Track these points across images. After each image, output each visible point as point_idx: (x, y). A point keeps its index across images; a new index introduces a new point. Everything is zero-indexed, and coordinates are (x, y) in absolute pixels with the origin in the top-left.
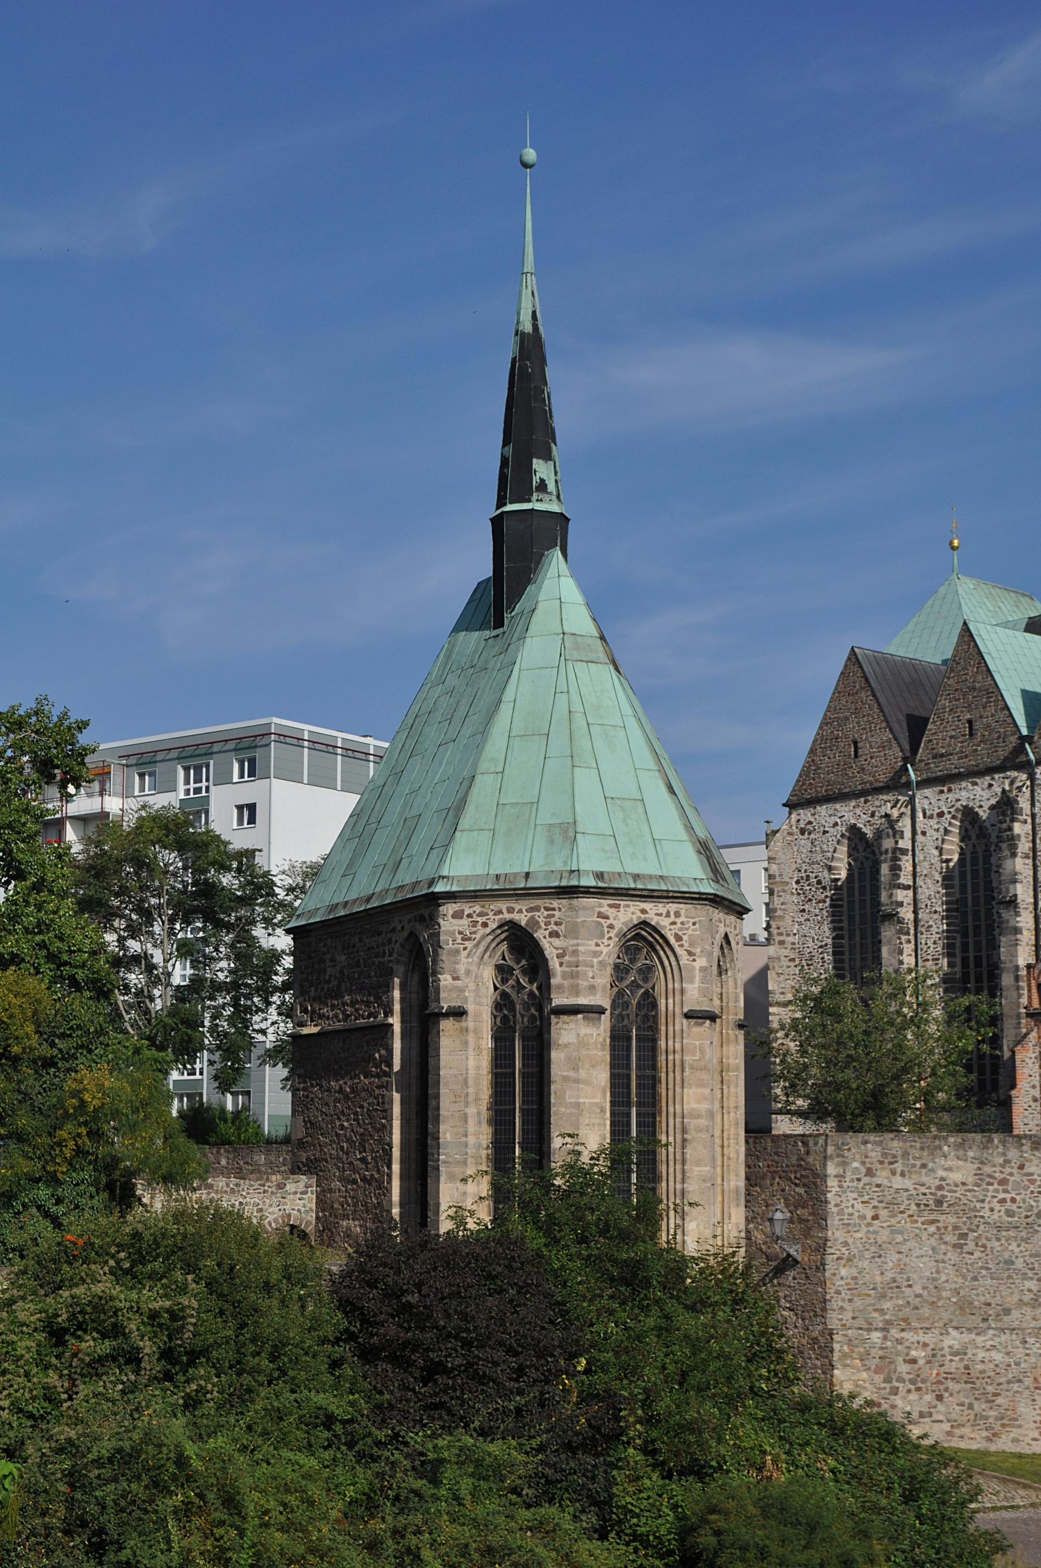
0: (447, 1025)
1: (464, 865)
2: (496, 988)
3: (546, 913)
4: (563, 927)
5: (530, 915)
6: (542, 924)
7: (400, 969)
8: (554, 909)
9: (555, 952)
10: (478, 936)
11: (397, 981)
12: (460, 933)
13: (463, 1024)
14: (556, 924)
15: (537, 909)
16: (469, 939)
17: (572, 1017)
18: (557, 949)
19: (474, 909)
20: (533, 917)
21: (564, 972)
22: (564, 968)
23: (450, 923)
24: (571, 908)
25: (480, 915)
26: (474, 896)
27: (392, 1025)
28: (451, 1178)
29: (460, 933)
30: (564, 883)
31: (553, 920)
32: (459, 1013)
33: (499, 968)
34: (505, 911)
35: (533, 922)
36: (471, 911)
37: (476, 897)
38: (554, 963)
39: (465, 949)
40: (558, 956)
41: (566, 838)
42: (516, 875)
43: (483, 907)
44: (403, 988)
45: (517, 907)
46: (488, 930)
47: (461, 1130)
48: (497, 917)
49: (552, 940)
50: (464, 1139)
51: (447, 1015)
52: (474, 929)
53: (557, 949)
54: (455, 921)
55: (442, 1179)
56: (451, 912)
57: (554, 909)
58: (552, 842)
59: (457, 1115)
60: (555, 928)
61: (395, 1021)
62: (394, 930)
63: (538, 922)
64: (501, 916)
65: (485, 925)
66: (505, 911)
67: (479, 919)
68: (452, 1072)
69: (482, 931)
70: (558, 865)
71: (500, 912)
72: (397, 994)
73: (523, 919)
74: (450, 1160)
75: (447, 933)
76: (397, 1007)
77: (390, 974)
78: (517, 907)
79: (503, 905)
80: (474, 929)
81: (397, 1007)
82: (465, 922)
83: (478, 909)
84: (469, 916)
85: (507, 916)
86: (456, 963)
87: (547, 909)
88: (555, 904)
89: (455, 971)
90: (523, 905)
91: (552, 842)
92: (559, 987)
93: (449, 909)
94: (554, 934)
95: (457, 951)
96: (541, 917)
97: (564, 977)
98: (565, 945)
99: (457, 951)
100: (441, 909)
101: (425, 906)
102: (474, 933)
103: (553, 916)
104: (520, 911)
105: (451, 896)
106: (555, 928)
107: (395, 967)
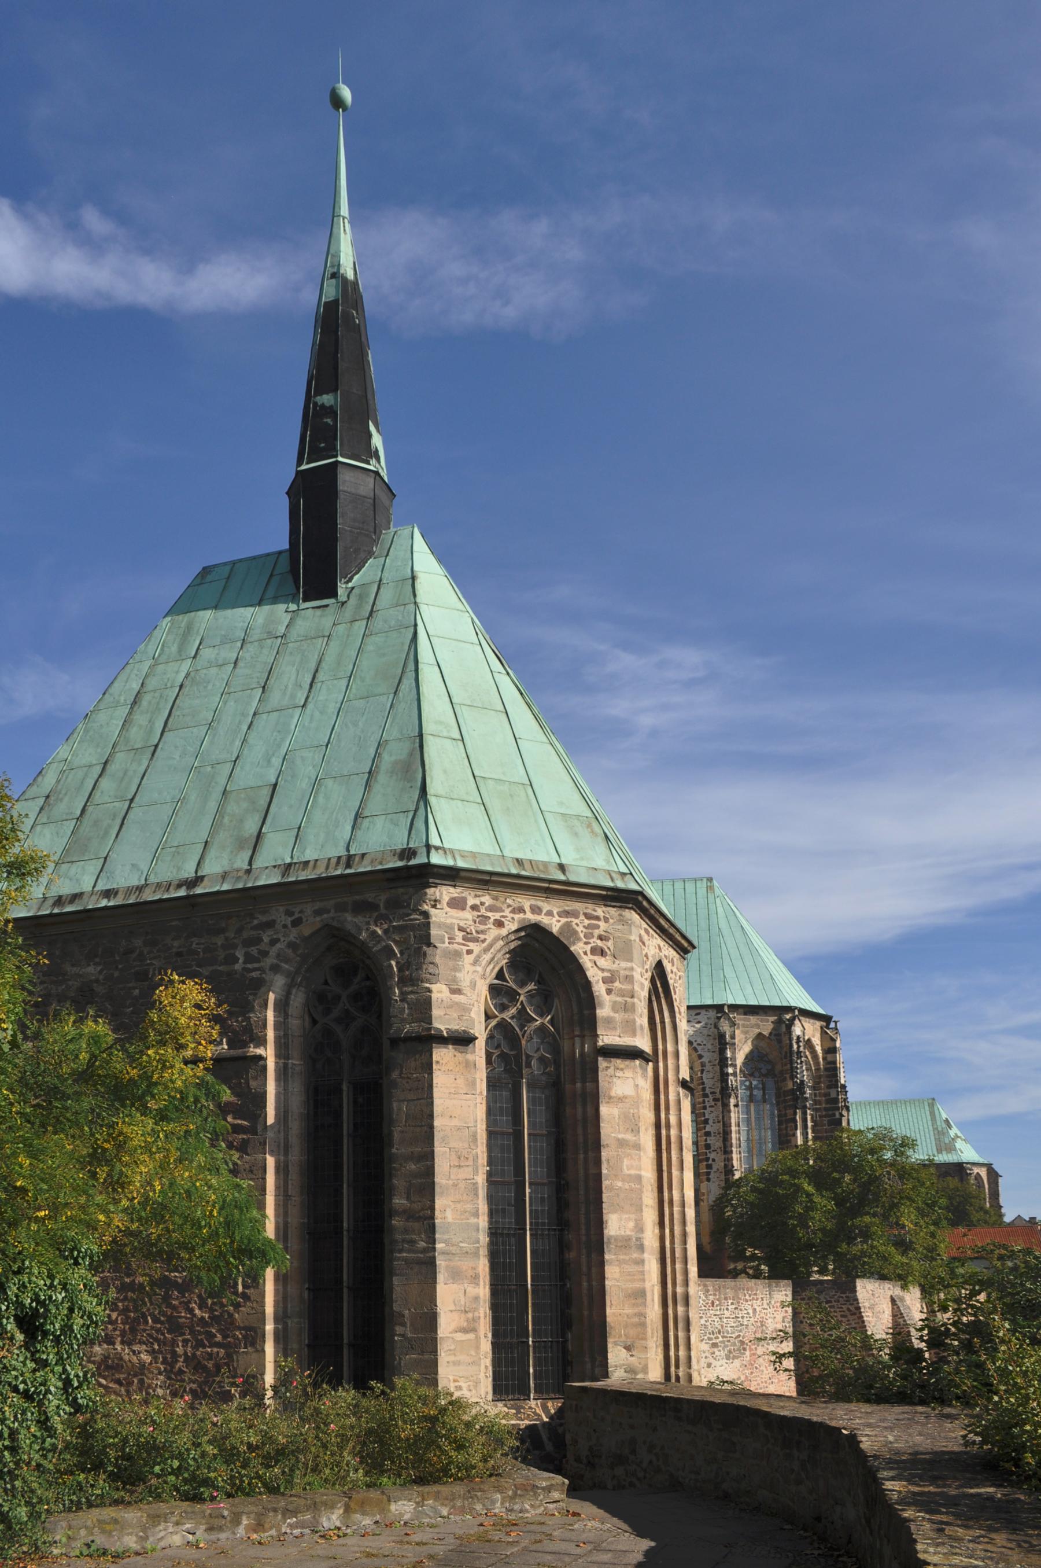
0: (443, 1056)
1: (458, 835)
2: (488, 1017)
3: (587, 922)
4: (610, 944)
5: (564, 920)
6: (582, 935)
7: (280, 981)
8: (598, 918)
9: (601, 974)
10: (490, 937)
11: (272, 997)
12: (461, 929)
13: (470, 1057)
14: (600, 938)
15: (575, 914)
16: (476, 940)
17: (628, 1062)
18: (603, 970)
19: (483, 899)
20: (568, 925)
21: (615, 1002)
22: (614, 997)
23: (446, 912)
24: (622, 920)
25: (491, 909)
27: (260, 1058)
28: (456, 1275)
30: (620, 884)
31: (596, 932)
32: (463, 1040)
33: (493, 990)
35: (567, 928)
36: (477, 901)
37: (486, 882)
38: (599, 989)
40: (605, 981)
42: (545, 864)
43: (496, 899)
44: (281, 1007)
45: (546, 907)
46: (504, 932)
47: (469, 1207)
48: (516, 916)
49: (596, 958)
50: (473, 1220)
51: (443, 1040)
52: (482, 927)
53: (603, 970)
54: (453, 912)
55: (441, 1278)
56: (446, 898)
57: (598, 918)
59: (462, 1185)
61: (269, 1053)
62: (270, 925)
63: (575, 932)
64: (522, 915)
65: (499, 924)
66: (527, 909)
67: (489, 914)
68: (455, 1122)
69: (494, 932)
71: (521, 910)
72: (270, 1015)
73: (555, 924)
74: (453, 1249)
75: (440, 926)
76: (271, 1034)
77: (259, 986)
79: (526, 902)
80: (482, 927)
81: (271, 1034)
82: (468, 915)
83: (487, 900)
85: (533, 918)
86: (457, 969)
87: (588, 916)
88: (600, 911)
89: (455, 980)
90: (555, 906)
92: (609, 1021)
93: (445, 893)
95: (457, 954)
96: (580, 925)
97: (615, 1007)
98: (615, 967)
99: (457, 954)
100: (430, 891)
101: (412, 878)
102: (483, 932)
103: (598, 927)
104: (550, 913)
105: (452, 875)
106: (599, 943)
107: (268, 977)
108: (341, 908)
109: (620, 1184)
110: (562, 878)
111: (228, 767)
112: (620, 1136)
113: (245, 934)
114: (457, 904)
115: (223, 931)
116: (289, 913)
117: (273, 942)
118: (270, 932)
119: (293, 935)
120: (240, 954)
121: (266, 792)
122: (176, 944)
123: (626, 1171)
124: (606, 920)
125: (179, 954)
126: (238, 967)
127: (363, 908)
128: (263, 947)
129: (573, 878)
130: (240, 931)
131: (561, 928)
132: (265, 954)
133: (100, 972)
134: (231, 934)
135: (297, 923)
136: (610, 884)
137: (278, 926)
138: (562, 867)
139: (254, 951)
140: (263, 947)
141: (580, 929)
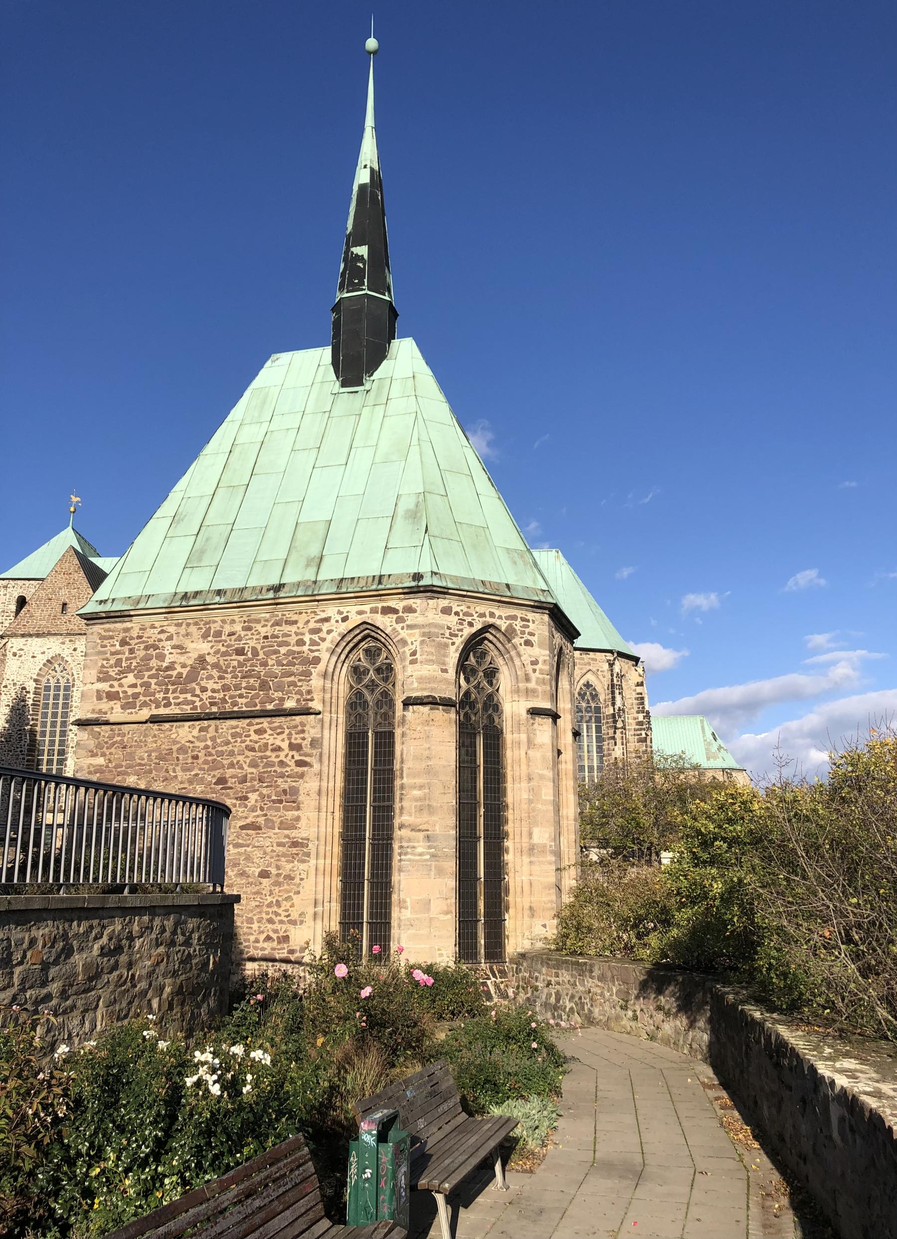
5: (508, 622)
6: (519, 632)
15: (514, 618)
16: (456, 636)
20: (511, 625)
26: (463, 595)
29: (449, 628)
31: (527, 630)
34: (487, 614)
39: (453, 644)
41: (525, 563)
48: (481, 619)
52: (461, 627)
57: (528, 621)
58: (515, 563)
60: (530, 638)
62: (327, 620)
63: (515, 630)
64: (484, 619)
65: (471, 624)
66: (487, 614)
67: (465, 618)
70: (530, 584)
78: (497, 613)
80: (461, 627)
84: (457, 614)
86: (445, 656)
87: (523, 619)
88: (530, 616)
91: (515, 563)
94: (528, 643)
95: (446, 646)
96: (518, 625)
103: (528, 627)
104: (500, 617)
108: (374, 611)
109: (540, 806)
110: (509, 594)
111: (296, 506)
112: (540, 772)
113: (312, 625)
114: (446, 611)
115: (296, 622)
116: (340, 613)
117: (329, 632)
118: (326, 624)
119: (344, 628)
120: (307, 638)
121: (322, 528)
122: (265, 629)
123: (544, 797)
124: (534, 622)
125: (266, 637)
126: (305, 648)
127: (387, 611)
128: (323, 634)
129: (515, 595)
130: (308, 621)
131: (507, 627)
132: (323, 640)
133: (212, 647)
134: (300, 625)
135: (345, 619)
136: (536, 598)
137: (333, 621)
138: (508, 586)
139: (315, 637)
140: (323, 634)
141: (517, 628)
